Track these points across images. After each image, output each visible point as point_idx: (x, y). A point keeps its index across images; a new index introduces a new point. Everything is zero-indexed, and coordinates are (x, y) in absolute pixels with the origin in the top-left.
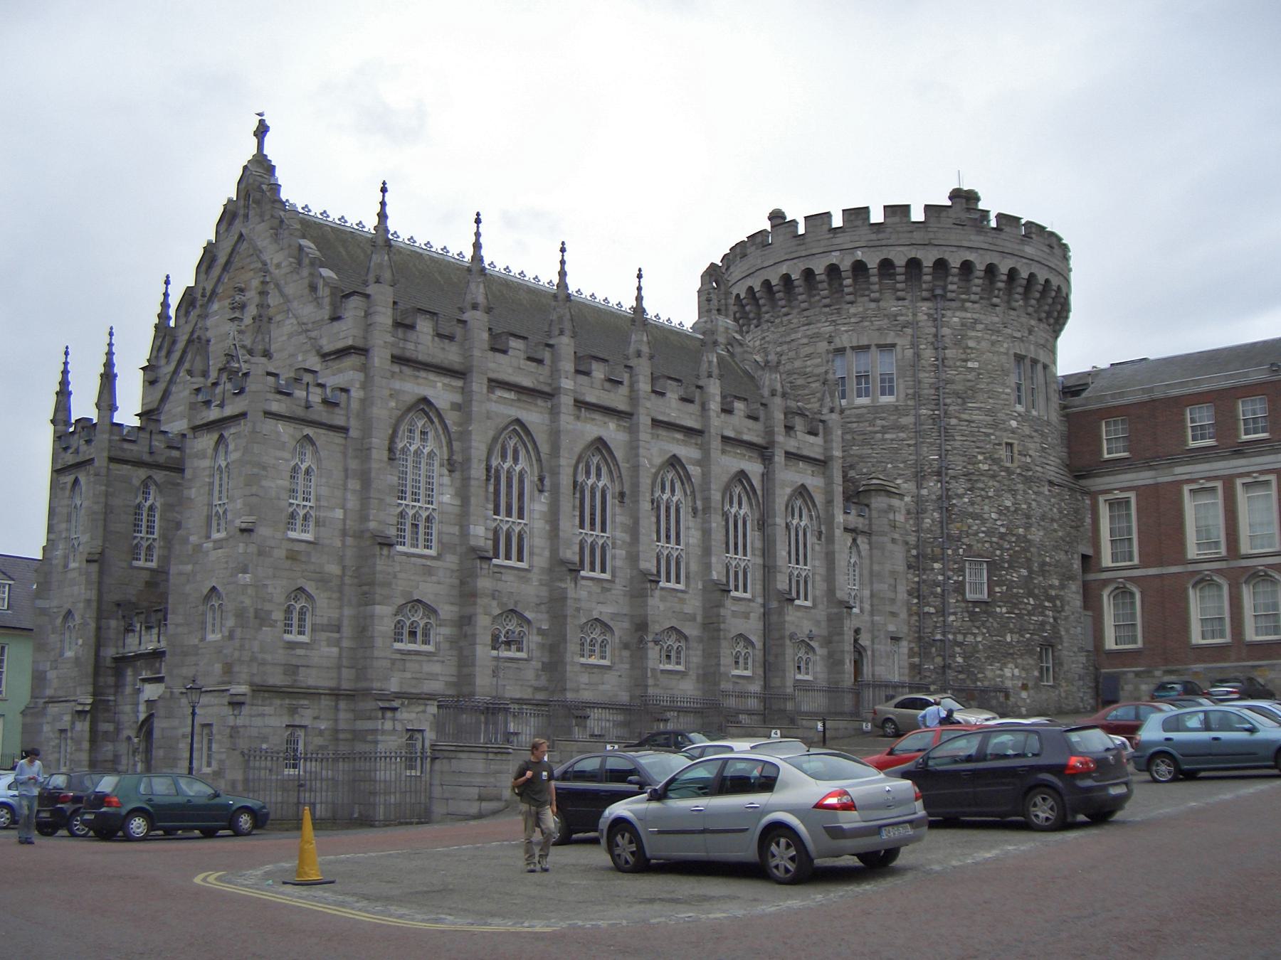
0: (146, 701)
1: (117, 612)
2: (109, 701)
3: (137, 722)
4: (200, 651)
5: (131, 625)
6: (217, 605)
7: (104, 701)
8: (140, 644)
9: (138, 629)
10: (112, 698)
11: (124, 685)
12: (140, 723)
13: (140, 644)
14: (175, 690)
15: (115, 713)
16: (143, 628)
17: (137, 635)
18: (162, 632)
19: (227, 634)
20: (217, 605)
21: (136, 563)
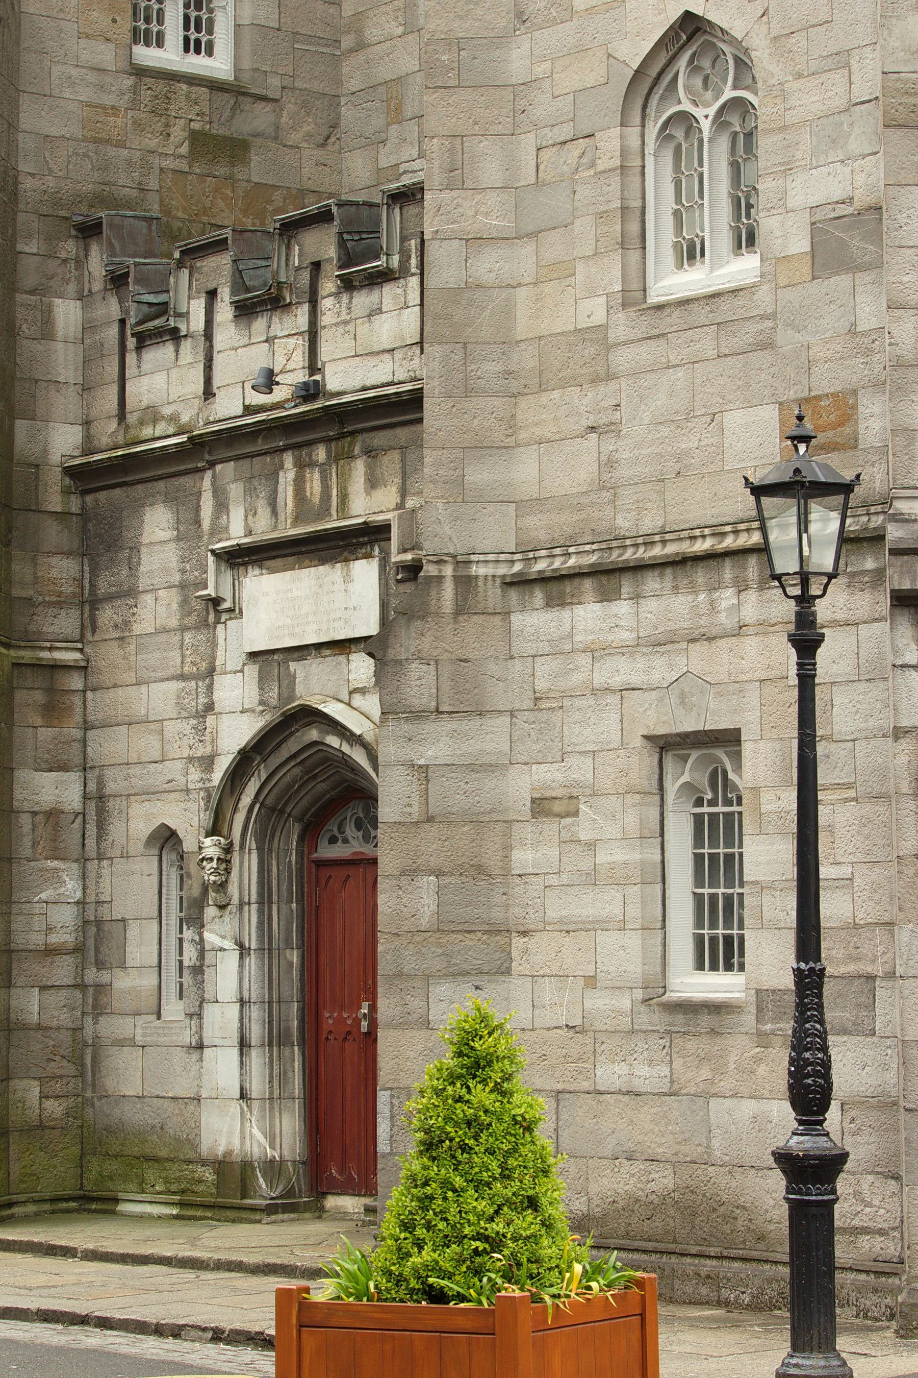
0: (254, 656)
1: (80, 262)
2: (56, 667)
3: (208, 763)
4: (621, 359)
5: (163, 309)
6: (705, 115)
7: (38, 666)
8: (208, 393)
9: (197, 322)
10: (71, 657)
11: (131, 593)
12: (223, 764)
13: (208, 393)
14: (474, 570)
15: (87, 726)
16: (224, 312)
17: (190, 352)
18: (326, 319)
19: (800, 244)
20: (705, 115)
21: (146, 55)
